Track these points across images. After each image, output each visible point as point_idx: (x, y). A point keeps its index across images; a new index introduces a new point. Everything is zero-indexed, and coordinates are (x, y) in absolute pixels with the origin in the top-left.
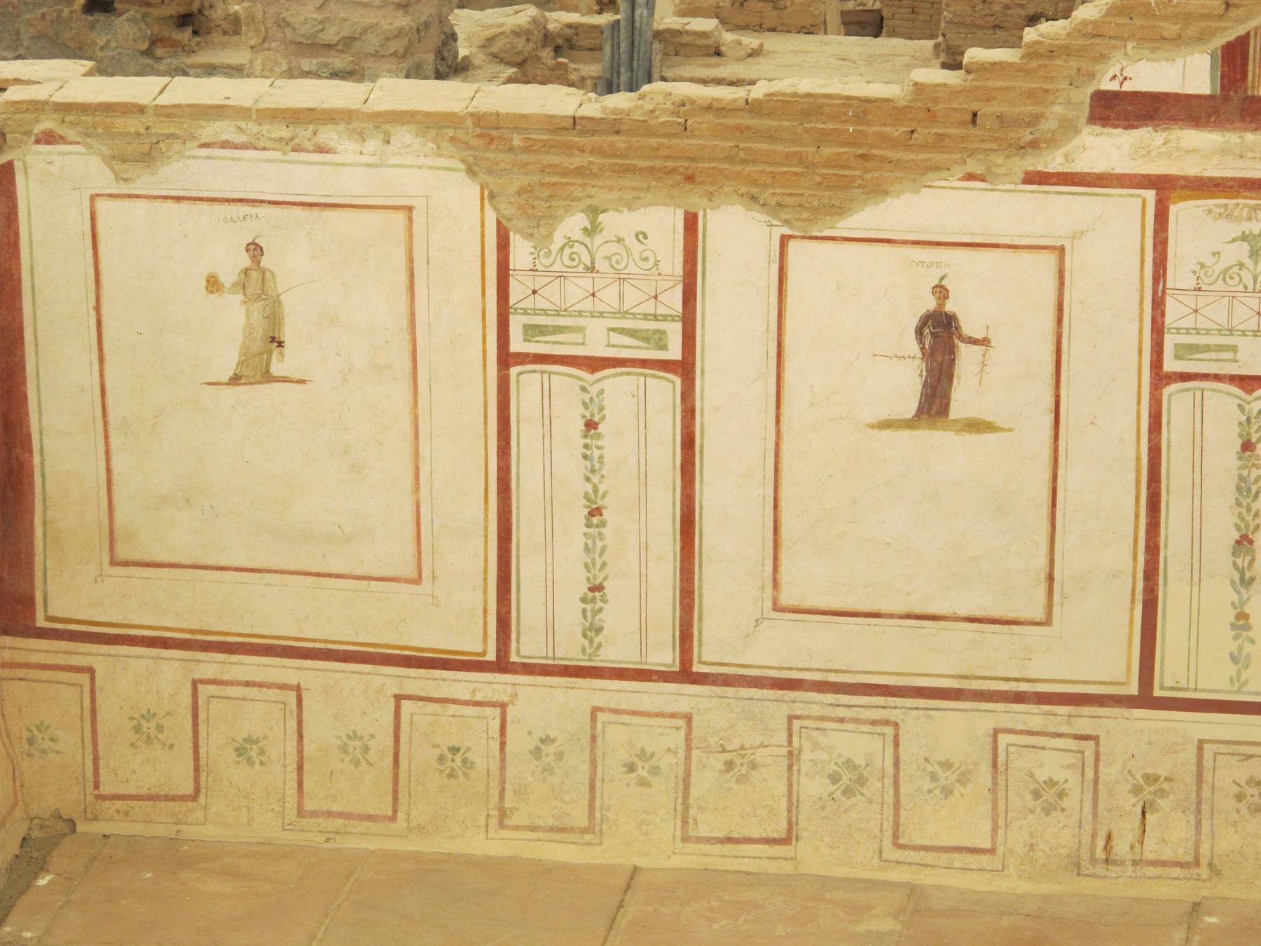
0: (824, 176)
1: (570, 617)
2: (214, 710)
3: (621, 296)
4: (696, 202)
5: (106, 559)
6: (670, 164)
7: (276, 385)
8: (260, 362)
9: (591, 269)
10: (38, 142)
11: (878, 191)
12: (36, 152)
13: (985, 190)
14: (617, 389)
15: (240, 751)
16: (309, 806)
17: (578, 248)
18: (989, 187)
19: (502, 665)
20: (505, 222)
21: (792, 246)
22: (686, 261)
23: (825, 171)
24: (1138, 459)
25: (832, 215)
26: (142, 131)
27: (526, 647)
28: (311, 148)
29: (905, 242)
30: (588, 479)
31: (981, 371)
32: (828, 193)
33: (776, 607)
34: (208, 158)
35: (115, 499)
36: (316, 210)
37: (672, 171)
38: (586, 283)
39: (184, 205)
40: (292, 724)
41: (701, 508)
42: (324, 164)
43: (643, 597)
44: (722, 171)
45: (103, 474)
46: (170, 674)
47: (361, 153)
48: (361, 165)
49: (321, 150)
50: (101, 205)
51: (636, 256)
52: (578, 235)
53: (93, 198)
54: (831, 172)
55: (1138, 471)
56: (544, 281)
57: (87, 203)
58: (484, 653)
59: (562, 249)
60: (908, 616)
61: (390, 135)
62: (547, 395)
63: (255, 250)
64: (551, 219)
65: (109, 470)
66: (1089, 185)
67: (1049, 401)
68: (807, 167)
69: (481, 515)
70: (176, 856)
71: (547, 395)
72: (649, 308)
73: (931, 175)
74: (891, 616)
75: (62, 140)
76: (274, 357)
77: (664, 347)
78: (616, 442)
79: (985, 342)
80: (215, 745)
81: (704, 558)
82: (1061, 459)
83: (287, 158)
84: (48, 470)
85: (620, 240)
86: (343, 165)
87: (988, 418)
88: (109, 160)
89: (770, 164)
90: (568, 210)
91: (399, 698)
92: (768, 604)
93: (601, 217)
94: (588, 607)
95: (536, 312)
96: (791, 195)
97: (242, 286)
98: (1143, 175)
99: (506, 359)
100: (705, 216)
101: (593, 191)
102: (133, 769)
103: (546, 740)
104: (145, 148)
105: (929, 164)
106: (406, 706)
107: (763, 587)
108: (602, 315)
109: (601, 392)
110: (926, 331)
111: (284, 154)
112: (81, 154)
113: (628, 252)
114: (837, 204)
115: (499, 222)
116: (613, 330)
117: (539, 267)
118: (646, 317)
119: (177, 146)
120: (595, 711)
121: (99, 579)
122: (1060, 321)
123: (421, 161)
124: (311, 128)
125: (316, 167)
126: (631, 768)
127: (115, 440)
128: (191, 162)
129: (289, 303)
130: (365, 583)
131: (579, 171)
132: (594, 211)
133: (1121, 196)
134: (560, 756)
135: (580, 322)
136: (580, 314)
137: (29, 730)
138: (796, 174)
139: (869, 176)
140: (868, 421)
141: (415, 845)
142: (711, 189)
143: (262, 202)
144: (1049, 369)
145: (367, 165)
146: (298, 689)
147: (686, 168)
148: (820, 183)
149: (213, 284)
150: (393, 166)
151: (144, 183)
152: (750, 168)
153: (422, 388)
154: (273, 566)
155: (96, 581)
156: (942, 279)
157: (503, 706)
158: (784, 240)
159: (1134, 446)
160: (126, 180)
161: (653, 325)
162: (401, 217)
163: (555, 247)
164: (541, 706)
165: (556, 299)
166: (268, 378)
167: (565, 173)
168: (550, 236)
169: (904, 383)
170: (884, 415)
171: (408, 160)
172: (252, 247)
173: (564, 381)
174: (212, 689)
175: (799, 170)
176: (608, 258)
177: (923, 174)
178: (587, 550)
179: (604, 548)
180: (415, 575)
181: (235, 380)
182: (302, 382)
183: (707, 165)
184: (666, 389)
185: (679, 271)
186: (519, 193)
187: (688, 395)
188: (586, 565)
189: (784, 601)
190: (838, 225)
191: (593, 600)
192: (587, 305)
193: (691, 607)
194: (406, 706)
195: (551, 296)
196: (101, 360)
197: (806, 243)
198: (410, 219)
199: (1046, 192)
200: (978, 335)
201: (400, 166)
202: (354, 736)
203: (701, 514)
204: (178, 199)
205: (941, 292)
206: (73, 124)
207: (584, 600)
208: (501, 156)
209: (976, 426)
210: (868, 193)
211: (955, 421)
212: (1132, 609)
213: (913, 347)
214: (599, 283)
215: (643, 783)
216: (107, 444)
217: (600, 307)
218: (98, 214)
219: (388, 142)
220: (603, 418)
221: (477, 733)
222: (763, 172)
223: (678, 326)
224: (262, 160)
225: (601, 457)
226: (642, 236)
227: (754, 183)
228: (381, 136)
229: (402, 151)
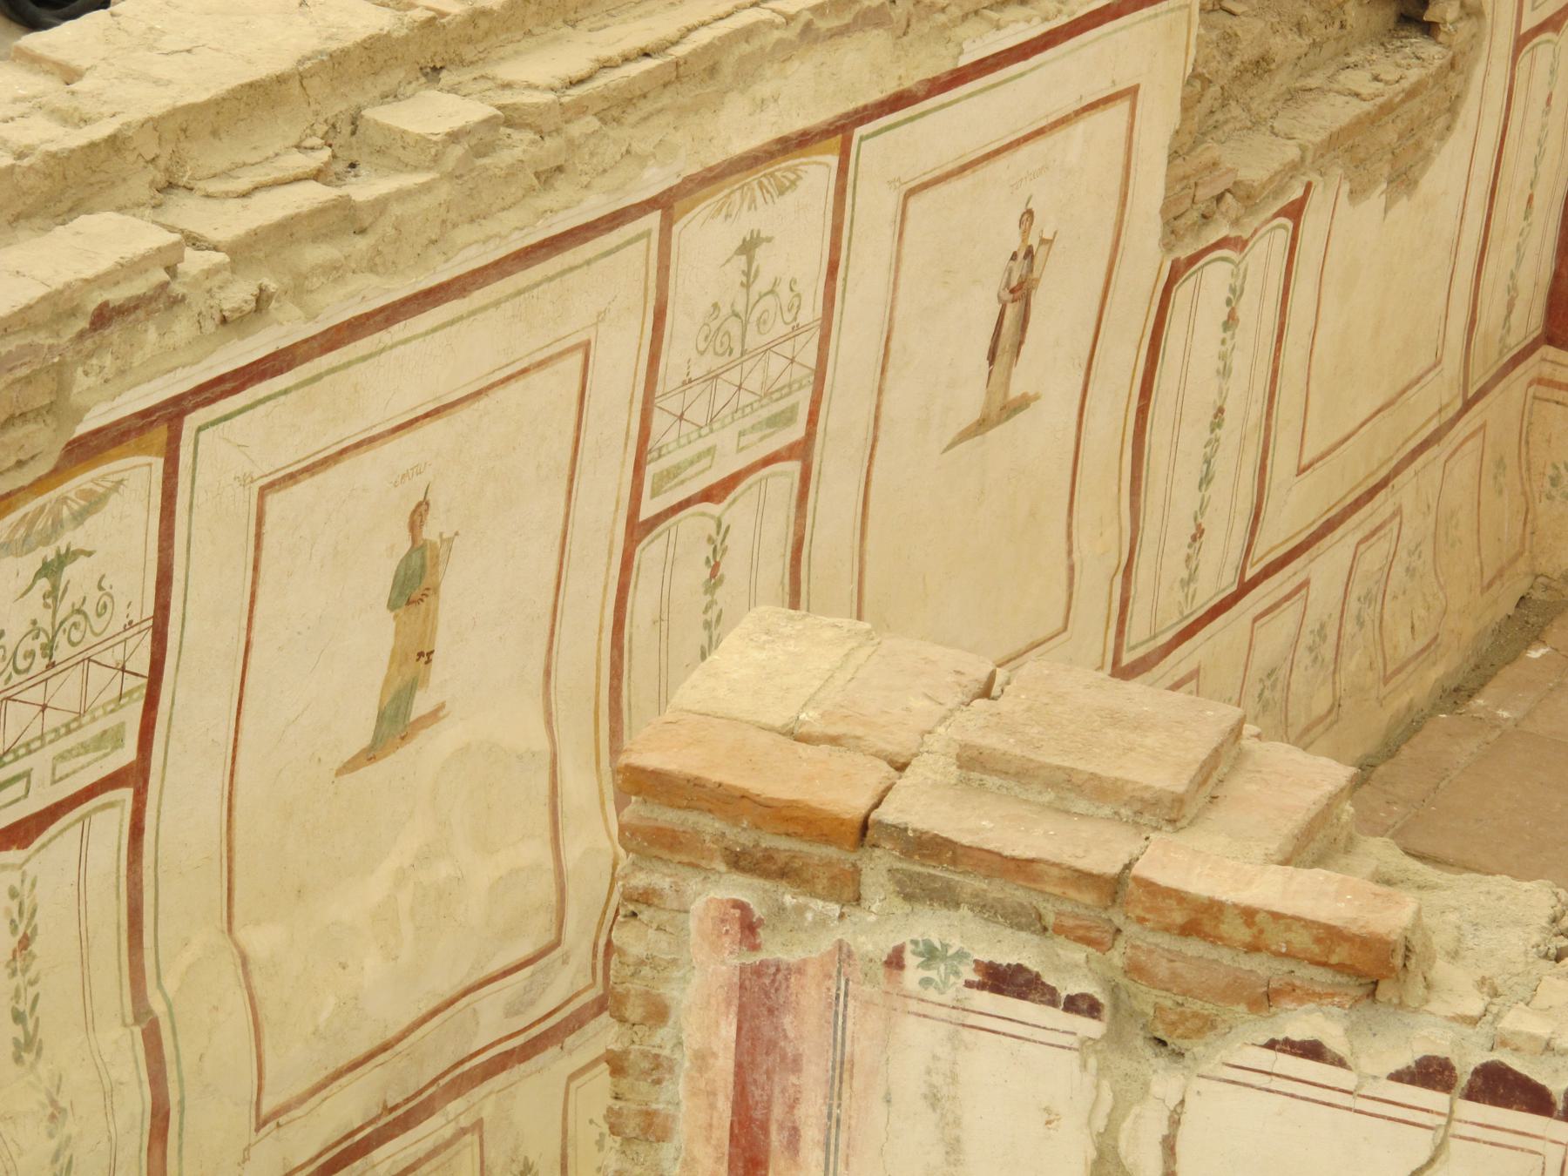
137: (1556, 467)
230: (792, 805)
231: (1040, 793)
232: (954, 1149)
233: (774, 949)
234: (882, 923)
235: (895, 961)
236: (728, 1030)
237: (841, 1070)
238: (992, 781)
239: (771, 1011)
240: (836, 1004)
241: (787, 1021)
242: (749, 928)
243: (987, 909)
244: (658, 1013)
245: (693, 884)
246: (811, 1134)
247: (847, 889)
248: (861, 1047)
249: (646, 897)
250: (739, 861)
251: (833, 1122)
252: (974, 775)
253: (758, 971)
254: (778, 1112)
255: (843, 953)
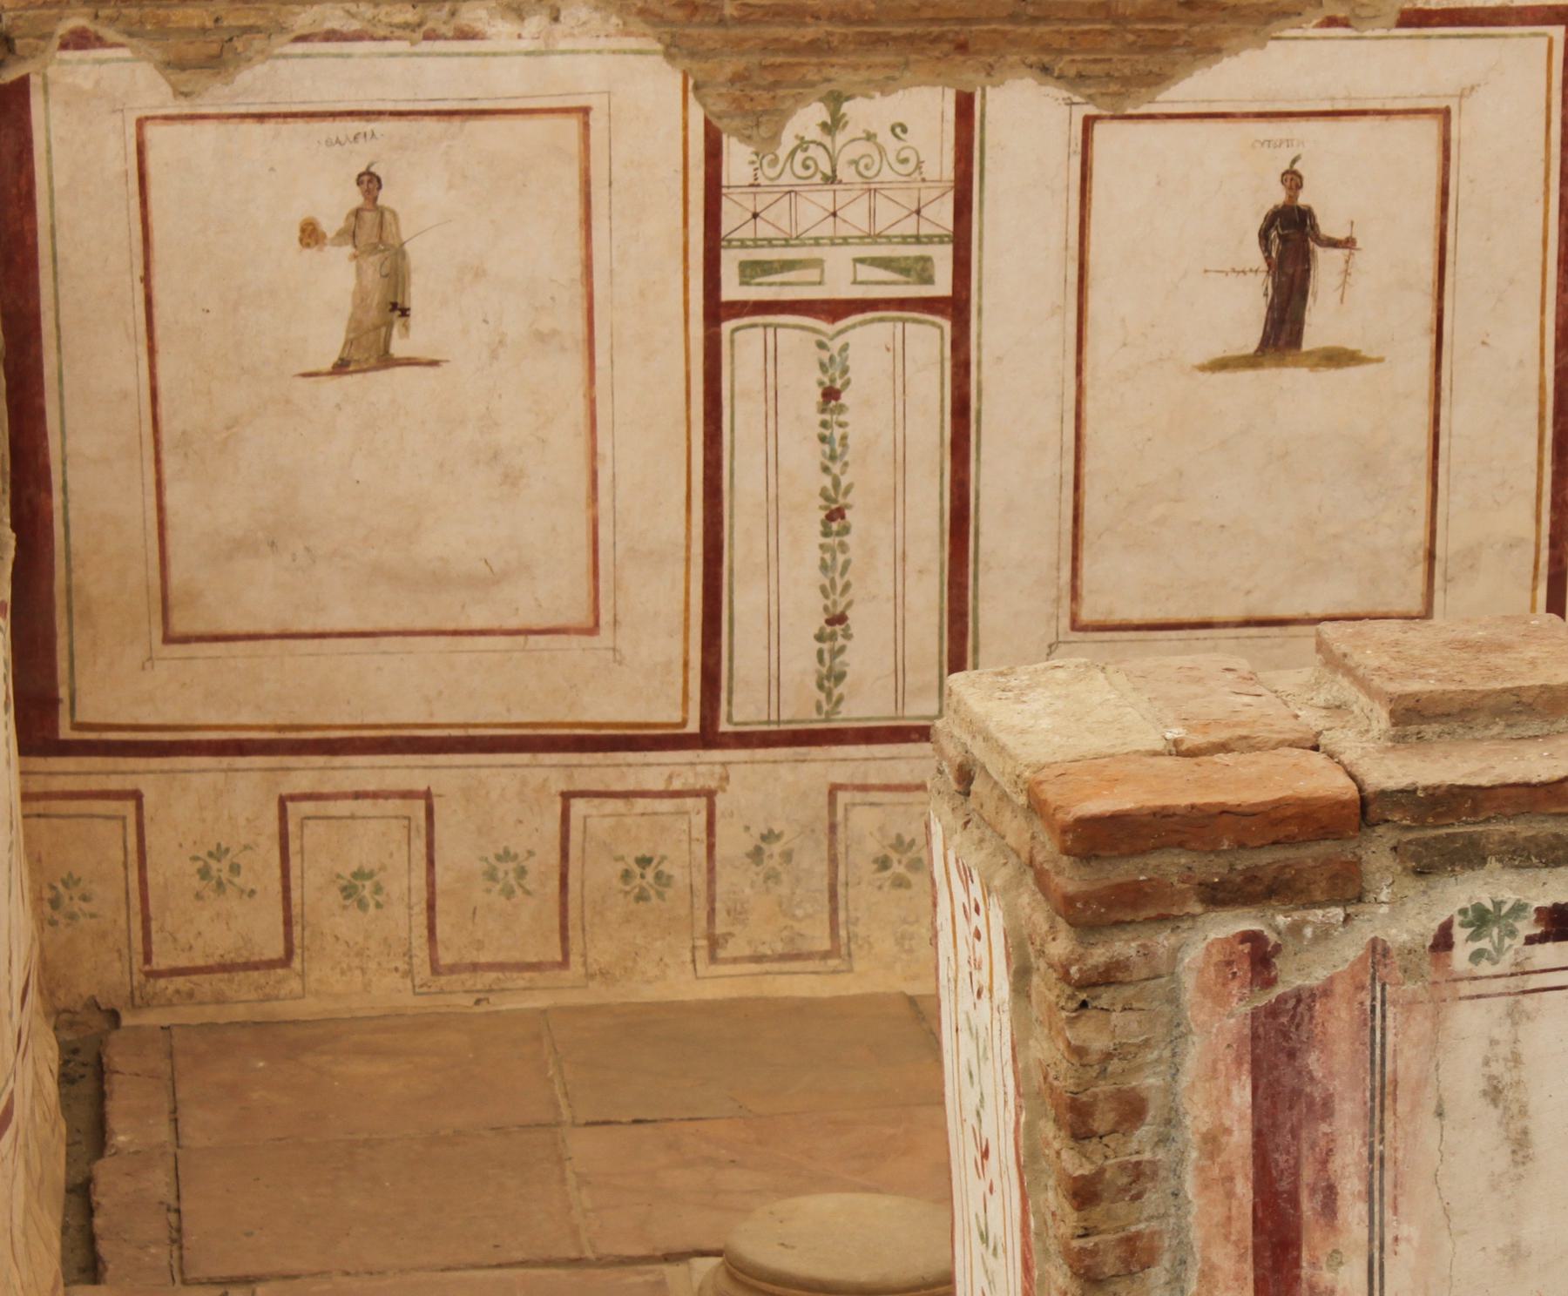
0: (1138, 33)
1: (800, 661)
2: (311, 838)
3: (872, 214)
4: (971, 78)
5: (157, 634)
6: (936, 30)
7: (399, 371)
8: (376, 338)
9: (831, 179)
10: (64, 46)
11: (1209, 50)
12: (62, 62)
13: (1349, 38)
14: (866, 341)
15: (348, 891)
16: (446, 958)
17: (814, 151)
18: (1354, 34)
19: (708, 738)
20: (715, 122)
21: (1099, 130)
22: (958, 161)
23: (1139, 26)
24: (1542, 387)
25: (1149, 85)
26: (209, 24)
27: (744, 708)
28: (450, 34)
29: (1246, 116)
30: (826, 469)
31: (1345, 282)
32: (1142, 57)
33: (1076, 626)
34: (306, 56)
35: (171, 549)
36: (456, 121)
37: (937, 39)
38: (825, 199)
39: (270, 126)
40: (420, 845)
41: (977, 498)
42: (468, 55)
43: (899, 626)
44: (1004, 34)
45: (152, 515)
46: (248, 788)
47: (520, 36)
48: (519, 53)
49: (464, 35)
50: (153, 132)
51: (891, 157)
52: (814, 133)
53: (141, 123)
54: (1146, 27)
55: (1542, 403)
56: (770, 198)
57: (132, 130)
58: (684, 724)
59: (793, 154)
60: (1247, 623)
61: (558, 10)
62: (772, 357)
63: (370, 181)
64: (780, 116)
65: (161, 508)
66: (1482, 24)
67: (1429, 316)
68: (1115, 22)
69: (682, 531)
70: (276, 1037)
71: (772, 357)
72: (908, 227)
73: (1276, 24)
74: (1225, 625)
75: (99, 42)
76: (395, 332)
77: (929, 280)
78: (864, 417)
79: (1348, 243)
80: (311, 883)
81: (981, 566)
82: (1445, 394)
83: (417, 49)
84: (72, 515)
85: (870, 137)
86: (495, 54)
87: (1352, 346)
88: (174, 65)
89: (1068, 21)
90: (800, 100)
91: (567, 796)
92: (1065, 622)
93: (846, 107)
94: (826, 646)
95: (757, 243)
96: (1095, 61)
97: (350, 234)
98: (1550, 7)
99: (716, 311)
100: (983, 96)
101: (831, 72)
102: (202, 929)
103: (769, 837)
104: (214, 49)
105: (1275, 8)
106: (579, 807)
107: (1058, 600)
108: (845, 241)
109: (845, 348)
110: (1273, 234)
111: (413, 44)
112: (126, 60)
113: (882, 151)
114: (1156, 69)
115: (707, 123)
116: (862, 261)
117: (762, 181)
118: (904, 240)
119: (258, 43)
120: (834, 790)
121: (148, 665)
122: (1444, 208)
123: (602, 43)
124: (447, 7)
125: (456, 61)
126: (884, 864)
127: (170, 465)
128: (280, 63)
129: (416, 253)
130: (521, 639)
131: (814, 47)
132: (835, 100)
133: (1522, 36)
134: (787, 856)
135: (816, 253)
136: (817, 242)
137: (53, 888)
138: (1103, 32)
139: (1197, 29)
140: (1197, 362)
141: (596, 994)
142: (991, 60)
143: (380, 113)
144: (1430, 275)
145: (528, 54)
146: (427, 796)
147: (957, 33)
148: (1134, 43)
149: (310, 234)
150: (563, 52)
151: (217, 96)
152: (1041, 29)
153: (601, 360)
154: (392, 626)
155: (143, 668)
156: (1294, 161)
157: (710, 795)
158: (1088, 123)
159: (1537, 368)
160: (186, 95)
161: (914, 251)
162: (572, 124)
163: (783, 152)
164: (761, 788)
165: (784, 224)
166: (387, 361)
167: (795, 49)
168: (775, 138)
169: (1244, 308)
170: (1218, 352)
171: (583, 44)
172: (366, 178)
173: (795, 336)
174: (308, 807)
175: (1106, 27)
176: (855, 163)
177: (1267, 23)
178: (824, 567)
179: (847, 564)
180: (591, 623)
181: (341, 367)
182: (434, 363)
183: (985, 28)
184: (928, 340)
185: (949, 174)
186: (732, 81)
187: (960, 342)
188: (823, 590)
189: (1086, 616)
190: (1159, 98)
191: (833, 637)
192: (826, 229)
193: (964, 635)
194: (579, 807)
195: (777, 220)
196: (152, 351)
197: (1116, 124)
198: (586, 126)
199: (1428, 37)
200: (1340, 234)
201: (573, 52)
202: (505, 856)
203: (977, 506)
204: (261, 117)
205: (1293, 180)
206: (112, 21)
207: (820, 638)
208: (707, 31)
209: (1337, 358)
210: (1194, 54)
211: (1309, 353)
212: (1534, 589)
213: (1254, 256)
214: (842, 198)
215: (900, 883)
216: (158, 472)
217: (844, 230)
218: (148, 145)
219: (556, 19)
220: (847, 383)
221: (675, 838)
222: (1059, 32)
223: (948, 250)
224: (381, 55)
225: (844, 438)
226: (899, 129)
227: (1047, 49)
228: (546, 11)
229: (576, 31)
230: (1278, 804)
231: (1486, 727)
232: (1520, 1145)
233: (1292, 977)
234: (1402, 914)
235: (1443, 941)
236: (1242, 1095)
237: (1381, 1096)
238: (1430, 730)
239: (1292, 1055)
240: (1370, 1023)
241: (1313, 1060)
242: (1260, 957)
243: (1522, 855)
244: (1132, 1110)
245: (1164, 940)
246: (1350, 1187)
247: (1348, 888)
248: (1405, 1059)
249: (1108, 976)
250: (1218, 896)
251: (1376, 1161)
252: (1413, 729)
253: (1273, 1011)
254: (1308, 1174)
255: (1378, 951)
